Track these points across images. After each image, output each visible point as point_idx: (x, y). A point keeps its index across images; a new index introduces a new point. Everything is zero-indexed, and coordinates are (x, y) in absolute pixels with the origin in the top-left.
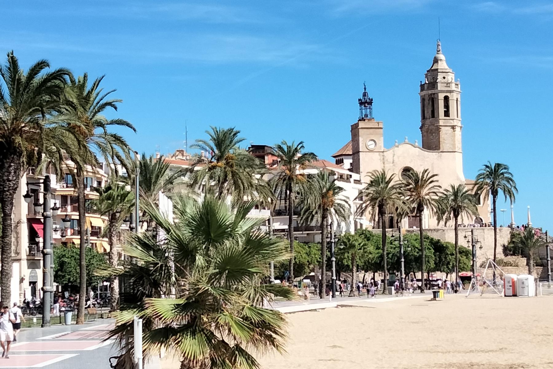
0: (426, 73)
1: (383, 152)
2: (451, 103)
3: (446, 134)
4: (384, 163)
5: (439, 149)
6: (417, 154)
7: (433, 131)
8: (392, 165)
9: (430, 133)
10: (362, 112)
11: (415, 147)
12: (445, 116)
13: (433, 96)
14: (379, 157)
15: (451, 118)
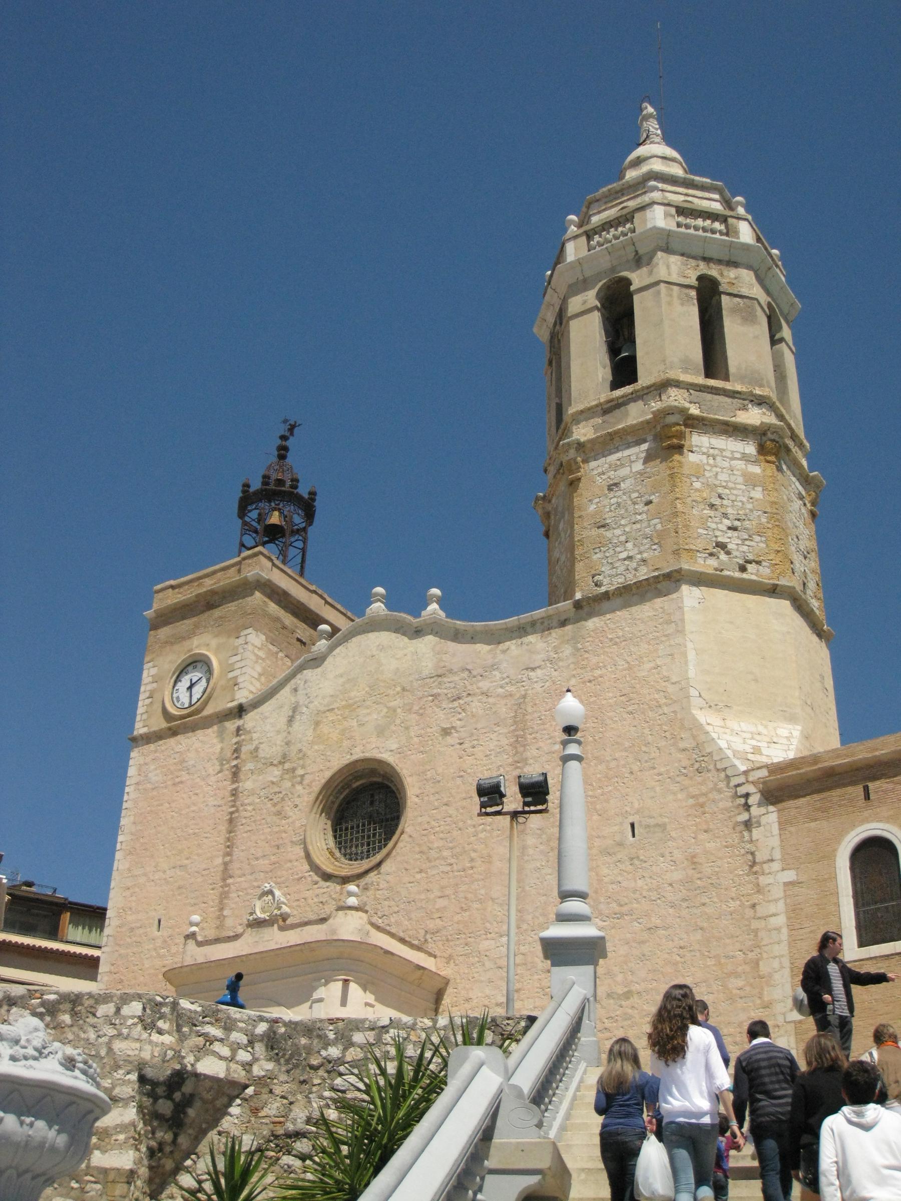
1: (241, 711)
3: (613, 486)
4: (235, 774)
5: (568, 594)
6: (428, 666)
11: (417, 633)
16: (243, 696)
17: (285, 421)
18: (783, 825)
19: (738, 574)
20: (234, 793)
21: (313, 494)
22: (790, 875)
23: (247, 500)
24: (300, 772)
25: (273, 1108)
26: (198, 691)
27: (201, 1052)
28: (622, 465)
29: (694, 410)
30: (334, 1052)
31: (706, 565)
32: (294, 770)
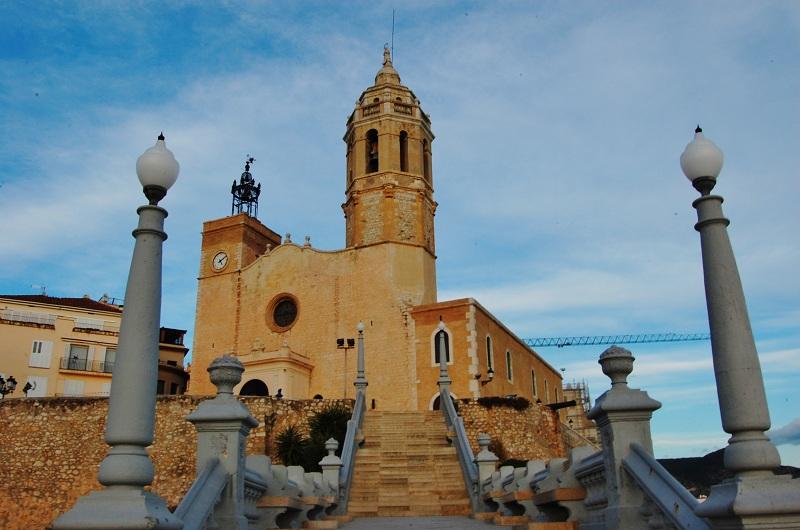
1: (240, 271)
2: (383, 142)
8: (253, 296)
15: (379, 172)
16: (239, 267)
19: (407, 242)
20: (239, 301)
21: (259, 185)
22: (417, 341)
23: (235, 188)
25: (294, 421)
26: (224, 262)
27: (277, 409)
29: (397, 183)
30: (307, 408)
31: (398, 238)
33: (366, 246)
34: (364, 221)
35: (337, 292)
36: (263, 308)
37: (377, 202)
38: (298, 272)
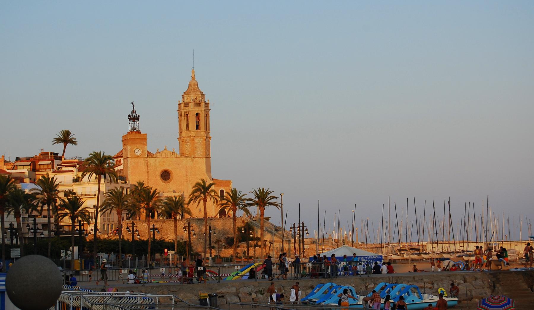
0: (183, 94)
7: (188, 141)
9: (185, 142)
10: (130, 126)
12: (196, 129)
13: (187, 113)
14: (144, 162)
15: (201, 131)
17: (133, 101)
18: (214, 187)
20: (148, 169)
24: (157, 168)
28: (198, 141)
32: (156, 168)
33: (197, 157)
34: (196, 148)
35: (187, 171)
36: (158, 173)
37: (201, 142)
38: (171, 162)
